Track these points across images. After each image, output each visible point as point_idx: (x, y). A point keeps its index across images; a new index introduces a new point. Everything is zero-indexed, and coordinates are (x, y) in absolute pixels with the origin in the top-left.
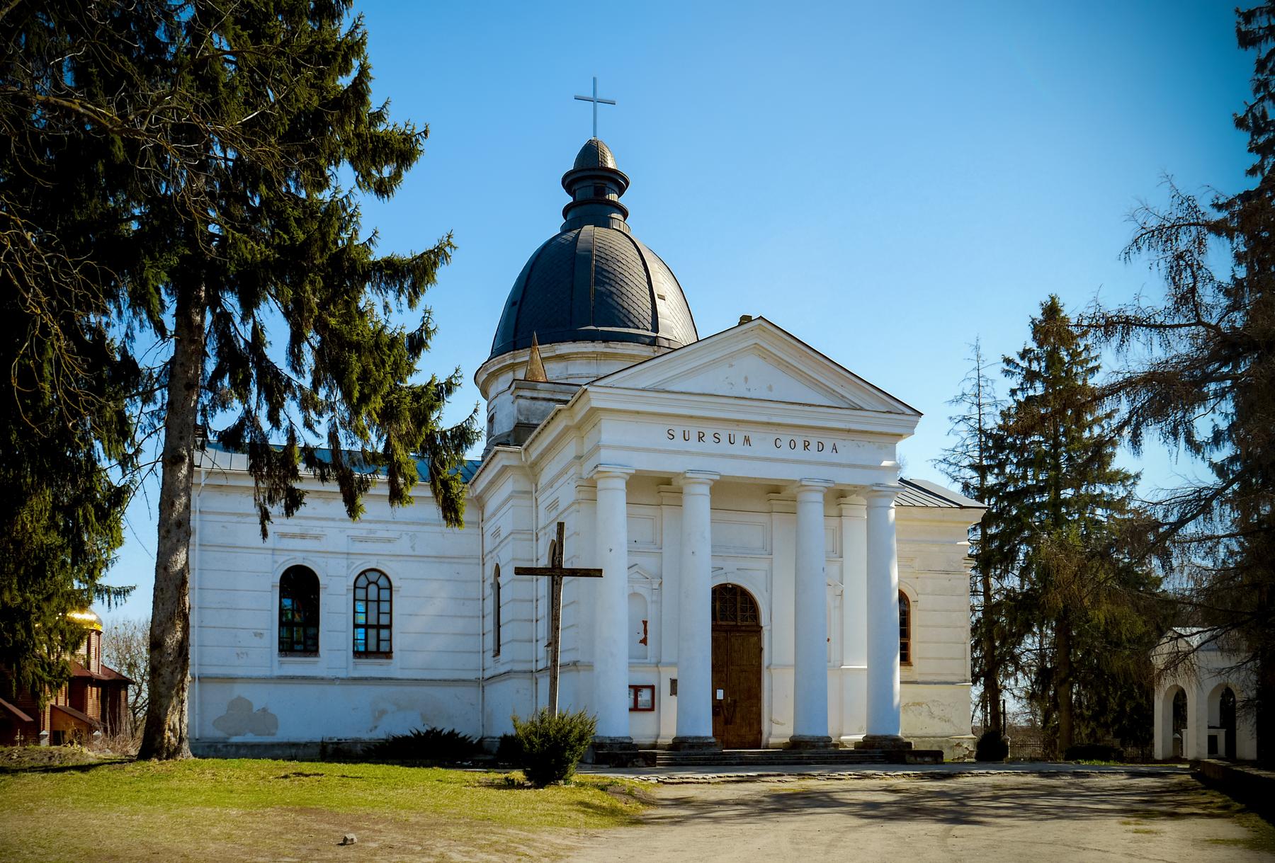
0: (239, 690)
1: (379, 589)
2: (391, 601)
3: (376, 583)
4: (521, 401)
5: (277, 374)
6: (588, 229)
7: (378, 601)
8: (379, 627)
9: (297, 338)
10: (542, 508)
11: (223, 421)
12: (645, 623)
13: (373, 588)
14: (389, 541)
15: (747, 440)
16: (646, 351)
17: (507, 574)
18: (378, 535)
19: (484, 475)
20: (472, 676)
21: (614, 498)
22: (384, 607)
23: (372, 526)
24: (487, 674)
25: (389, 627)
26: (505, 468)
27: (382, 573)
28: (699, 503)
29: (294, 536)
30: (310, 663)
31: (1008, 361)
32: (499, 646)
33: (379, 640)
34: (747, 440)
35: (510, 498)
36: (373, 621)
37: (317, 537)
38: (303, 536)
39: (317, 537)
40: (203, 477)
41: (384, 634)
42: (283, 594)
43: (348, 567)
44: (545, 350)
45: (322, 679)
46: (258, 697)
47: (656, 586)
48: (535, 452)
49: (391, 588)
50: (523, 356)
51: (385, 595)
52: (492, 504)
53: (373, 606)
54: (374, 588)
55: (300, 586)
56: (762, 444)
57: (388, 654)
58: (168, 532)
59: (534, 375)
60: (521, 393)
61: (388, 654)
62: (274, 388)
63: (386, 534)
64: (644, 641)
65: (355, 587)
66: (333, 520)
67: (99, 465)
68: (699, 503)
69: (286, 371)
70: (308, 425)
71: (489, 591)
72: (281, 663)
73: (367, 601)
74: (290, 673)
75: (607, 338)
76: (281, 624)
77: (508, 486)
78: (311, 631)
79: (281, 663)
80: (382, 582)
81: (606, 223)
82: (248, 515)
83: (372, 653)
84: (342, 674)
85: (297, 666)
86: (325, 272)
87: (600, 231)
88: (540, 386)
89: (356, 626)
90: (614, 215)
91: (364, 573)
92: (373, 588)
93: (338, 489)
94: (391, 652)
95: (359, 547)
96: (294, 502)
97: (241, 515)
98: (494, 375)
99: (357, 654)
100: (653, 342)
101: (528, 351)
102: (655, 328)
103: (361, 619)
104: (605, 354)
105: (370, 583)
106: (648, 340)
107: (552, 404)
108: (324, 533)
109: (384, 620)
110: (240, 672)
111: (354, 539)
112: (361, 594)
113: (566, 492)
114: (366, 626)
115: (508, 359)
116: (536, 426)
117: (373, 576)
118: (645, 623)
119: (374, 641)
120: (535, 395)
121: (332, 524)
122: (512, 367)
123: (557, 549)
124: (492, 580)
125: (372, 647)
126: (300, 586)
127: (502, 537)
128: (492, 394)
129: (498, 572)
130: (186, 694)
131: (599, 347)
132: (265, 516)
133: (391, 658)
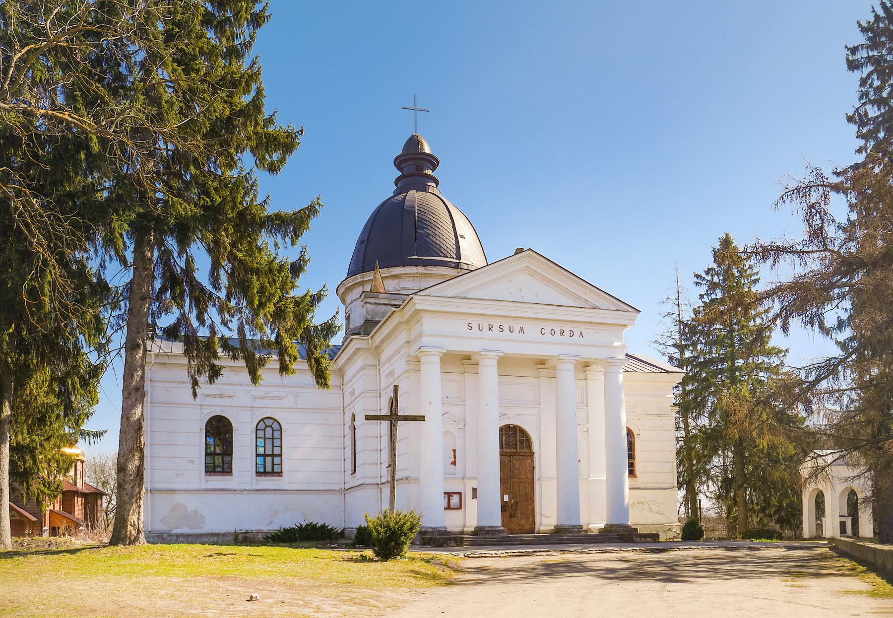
0: (179, 498)
1: (273, 430)
2: (281, 438)
3: (271, 427)
4: (368, 306)
5: (202, 290)
6: (412, 193)
7: (273, 438)
8: (273, 455)
9: (216, 266)
10: (383, 376)
11: (166, 321)
12: (454, 451)
13: (269, 430)
14: (280, 398)
16: (452, 272)
17: (360, 420)
19: (343, 354)
20: (337, 487)
21: (432, 368)
22: (277, 442)
23: (268, 389)
24: (347, 487)
25: (280, 455)
26: (358, 349)
27: (275, 420)
28: (489, 370)
29: (215, 396)
30: (224, 480)
32: (355, 467)
33: (273, 464)
35: (361, 369)
36: (269, 452)
38: (221, 396)
40: (153, 358)
41: (277, 460)
42: (208, 434)
44: (385, 272)
46: (192, 503)
47: (461, 427)
48: (378, 338)
49: (281, 430)
50: (369, 276)
51: (277, 434)
52: (349, 373)
53: (269, 442)
54: (270, 430)
55: (219, 430)
58: (130, 394)
59: (376, 288)
60: (368, 300)
61: (280, 474)
62: (201, 299)
63: (277, 394)
64: (454, 463)
65: (257, 430)
66: (241, 385)
67: (82, 351)
68: (489, 370)
69: (209, 287)
70: (224, 323)
71: (348, 431)
73: (265, 438)
74: (214, 487)
75: (426, 264)
76: (207, 454)
77: (359, 362)
78: (227, 459)
79: (207, 480)
80: (275, 426)
81: (424, 189)
82: (184, 383)
84: (248, 487)
85: (218, 481)
86: (234, 222)
87: (420, 194)
88: (381, 296)
89: (257, 455)
90: (429, 184)
91: (262, 420)
92: (269, 430)
93: (244, 365)
94: (281, 472)
95: (259, 403)
96: (215, 373)
97: (179, 383)
98: (350, 289)
99: (258, 473)
100: (457, 266)
101: (372, 273)
102: (459, 256)
103: (261, 450)
104: (425, 274)
105: (266, 427)
106: (453, 265)
107: (389, 307)
108: (237, 395)
109: (277, 451)
110: (178, 487)
111: (255, 398)
112: (261, 434)
113: (400, 365)
114: (265, 455)
115: (359, 278)
116: (378, 322)
117: (269, 422)
118: (454, 451)
119: (269, 465)
120: (377, 301)
121: (241, 388)
122: (362, 283)
123: (394, 403)
124: (350, 424)
125: (269, 469)
126: (219, 430)
127: (356, 395)
128: (348, 300)
129: (354, 419)
130: (142, 501)
131: (421, 270)
132: (195, 383)
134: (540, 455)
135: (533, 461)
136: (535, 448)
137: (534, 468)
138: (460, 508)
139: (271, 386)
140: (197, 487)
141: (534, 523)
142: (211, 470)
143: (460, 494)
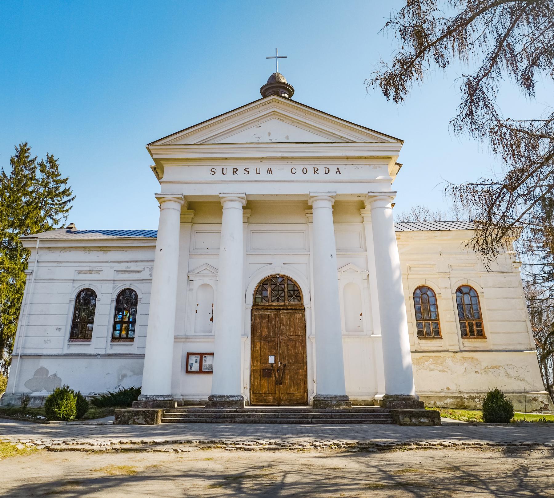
0: (44, 363)
12: (213, 305)
14: (138, 272)
18: (132, 269)
29: (86, 272)
30: (84, 345)
38: (90, 272)
39: (98, 272)
43: (114, 288)
45: (90, 355)
57: (132, 339)
66: (107, 262)
72: (69, 346)
79: (69, 346)
84: (103, 352)
85: (79, 347)
111: (118, 272)
118: (213, 305)
126: (85, 301)
133: (133, 341)
139: (131, 262)
140: (59, 352)
142: (73, 336)
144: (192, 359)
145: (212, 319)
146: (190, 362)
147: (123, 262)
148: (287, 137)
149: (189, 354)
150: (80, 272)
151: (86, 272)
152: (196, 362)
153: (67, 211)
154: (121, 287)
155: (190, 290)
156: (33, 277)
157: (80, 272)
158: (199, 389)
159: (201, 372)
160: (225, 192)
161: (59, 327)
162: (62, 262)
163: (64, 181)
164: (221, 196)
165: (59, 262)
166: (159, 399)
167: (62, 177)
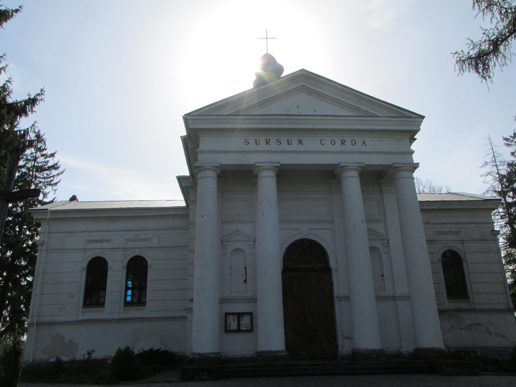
12: (246, 268)
14: (147, 240)
15: (300, 142)
23: (137, 233)
29: (96, 241)
31: (506, 139)
34: (300, 142)
37: (108, 241)
38: (101, 241)
39: (108, 241)
47: (252, 243)
56: (311, 143)
57: (144, 304)
64: (245, 281)
66: (117, 231)
72: (83, 312)
79: (83, 312)
83: (136, 303)
84: (116, 317)
85: (93, 314)
111: (128, 240)
118: (246, 268)
121: (116, 233)
126: (97, 269)
134: (336, 270)
135: (331, 277)
136: (332, 264)
137: (332, 284)
138: (251, 330)
139: (140, 230)
141: (336, 346)
143: (251, 314)
144: (230, 319)
145: (245, 281)
146: (228, 322)
147: (132, 230)
148: (315, 111)
149: (227, 314)
150: (91, 241)
151: (96, 241)
152: (234, 321)
153: (56, 184)
154: (131, 254)
155: (223, 254)
156: (44, 247)
157: (91, 241)
158: (239, 347)
159: (239, 330)
160: (260, 161)
161: (73, 295)
162: (73, 232)
163: (52, 155)
164: (257, 165)
165: (70, 232)
166: (212, 356)
167: (49, 152)
